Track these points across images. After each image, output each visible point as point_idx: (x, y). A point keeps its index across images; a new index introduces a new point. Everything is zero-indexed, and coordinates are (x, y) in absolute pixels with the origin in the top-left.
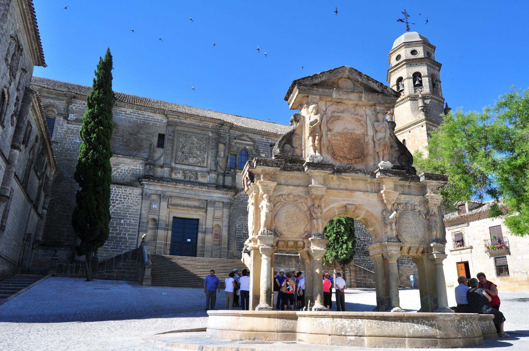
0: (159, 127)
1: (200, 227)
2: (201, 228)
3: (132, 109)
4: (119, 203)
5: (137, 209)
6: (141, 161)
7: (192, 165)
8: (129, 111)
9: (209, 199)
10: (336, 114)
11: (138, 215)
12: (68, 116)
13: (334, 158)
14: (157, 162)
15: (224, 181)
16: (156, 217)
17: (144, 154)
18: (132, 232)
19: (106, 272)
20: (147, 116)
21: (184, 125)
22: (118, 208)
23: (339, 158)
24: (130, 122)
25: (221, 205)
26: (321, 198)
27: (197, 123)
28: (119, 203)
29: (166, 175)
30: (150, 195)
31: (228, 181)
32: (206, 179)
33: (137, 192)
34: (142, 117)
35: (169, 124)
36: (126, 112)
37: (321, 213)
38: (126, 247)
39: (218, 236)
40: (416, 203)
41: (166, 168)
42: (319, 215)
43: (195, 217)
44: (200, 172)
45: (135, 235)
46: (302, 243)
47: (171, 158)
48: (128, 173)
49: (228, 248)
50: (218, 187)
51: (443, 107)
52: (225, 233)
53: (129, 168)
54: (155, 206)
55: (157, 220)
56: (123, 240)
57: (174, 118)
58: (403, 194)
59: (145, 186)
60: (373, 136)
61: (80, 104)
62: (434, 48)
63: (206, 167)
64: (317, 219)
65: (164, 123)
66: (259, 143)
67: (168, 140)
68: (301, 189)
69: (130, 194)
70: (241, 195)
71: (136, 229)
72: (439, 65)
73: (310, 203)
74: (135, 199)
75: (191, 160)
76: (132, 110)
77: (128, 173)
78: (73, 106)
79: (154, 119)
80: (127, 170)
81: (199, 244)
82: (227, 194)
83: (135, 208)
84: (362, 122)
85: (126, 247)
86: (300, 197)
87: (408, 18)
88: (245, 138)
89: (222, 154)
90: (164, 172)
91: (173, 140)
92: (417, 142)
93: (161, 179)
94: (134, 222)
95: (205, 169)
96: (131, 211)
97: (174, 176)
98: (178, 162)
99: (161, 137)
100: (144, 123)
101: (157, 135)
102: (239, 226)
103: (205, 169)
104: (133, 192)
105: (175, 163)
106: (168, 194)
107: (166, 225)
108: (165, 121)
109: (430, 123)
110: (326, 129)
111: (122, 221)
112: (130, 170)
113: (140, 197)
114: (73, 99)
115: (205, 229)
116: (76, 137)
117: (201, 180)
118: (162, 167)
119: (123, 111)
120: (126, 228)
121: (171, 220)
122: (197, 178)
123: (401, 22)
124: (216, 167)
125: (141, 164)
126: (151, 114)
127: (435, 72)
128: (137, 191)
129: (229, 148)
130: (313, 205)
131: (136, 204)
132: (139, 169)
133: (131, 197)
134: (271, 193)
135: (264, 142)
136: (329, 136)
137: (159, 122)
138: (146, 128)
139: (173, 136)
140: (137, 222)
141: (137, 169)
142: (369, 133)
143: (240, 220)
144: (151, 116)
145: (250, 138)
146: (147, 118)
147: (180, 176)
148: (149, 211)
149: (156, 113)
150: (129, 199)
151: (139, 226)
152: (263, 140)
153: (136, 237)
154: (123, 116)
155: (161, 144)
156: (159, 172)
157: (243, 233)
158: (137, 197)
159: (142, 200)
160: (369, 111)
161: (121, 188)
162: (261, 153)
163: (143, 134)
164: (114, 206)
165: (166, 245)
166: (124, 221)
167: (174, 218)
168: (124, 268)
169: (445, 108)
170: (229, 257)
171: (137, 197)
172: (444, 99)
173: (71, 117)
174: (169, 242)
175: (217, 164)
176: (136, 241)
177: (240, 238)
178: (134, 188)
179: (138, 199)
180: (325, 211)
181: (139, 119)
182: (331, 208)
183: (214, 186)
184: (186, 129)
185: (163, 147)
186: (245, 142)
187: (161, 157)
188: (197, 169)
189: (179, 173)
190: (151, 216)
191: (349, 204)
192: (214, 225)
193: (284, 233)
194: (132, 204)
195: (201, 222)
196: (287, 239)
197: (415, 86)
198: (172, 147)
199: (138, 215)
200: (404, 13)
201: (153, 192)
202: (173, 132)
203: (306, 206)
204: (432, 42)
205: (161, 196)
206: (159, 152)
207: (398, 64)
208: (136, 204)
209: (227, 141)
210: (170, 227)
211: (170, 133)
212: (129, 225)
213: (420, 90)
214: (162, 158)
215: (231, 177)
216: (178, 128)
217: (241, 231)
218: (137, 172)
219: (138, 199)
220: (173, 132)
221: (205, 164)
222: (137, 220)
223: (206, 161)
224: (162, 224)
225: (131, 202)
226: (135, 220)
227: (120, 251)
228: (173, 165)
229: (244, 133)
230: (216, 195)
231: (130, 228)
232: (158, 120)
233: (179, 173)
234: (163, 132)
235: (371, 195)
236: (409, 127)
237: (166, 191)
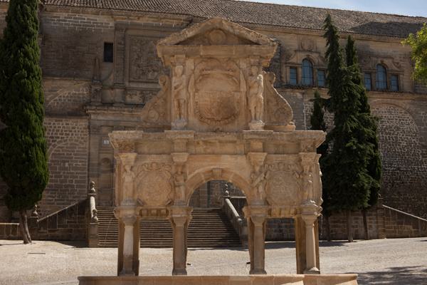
3: (67, 12)
4: (61, 142)
6: (84, 83)
7: (153, 82)
8: (63, 15)
10: (205, 72)
13: (201, 121)
19: (50, 231)
20: (88, 19)
22: (59, 147)
23: (206, 120)
24: (65, 31)
26: (184, 166)
27: (154, 23)
28: (61, 142)
29: (118, 99)
33: (82, 125)
34: (81, 22)
35: (117, 28)
36: (59, 17)
37: (185, 180)
38: (74, 197)
40: (291, 163)
41: (117, 90)
42: (182, 182)
45: (84, 182)
46: (165, 211)
47: (124, 75)
49: (209, 193)
53: (69, 93)
56: (70, 189)
57: (123, 19)
58: (275, 154)
59: (92, 117)
60: (246, 92)
64: (179, 186)
65: (111, 27)
67: (118, 50)
68: (164, 156)
69: (73, 128)
71: (85, 173)
73: (173, 171)
75: (150, 75)
76: (66, 15)
80: (67, 96)
84: (234, 78)
85: (74, 197)
86: (164, 164)
96: (77, 151)
97: (128, 100)
98: (132, 79)
99: (108, 46)
101: (103, 45)
104: (76, 125)
105: (130, 82)
108: (112, 24)
110: (194, 90)
111: (67, 165)
112: (71, 97)
118: (112, 88)
119: (55, 17)
120: (72, 173)
125: (85, 86)
126: (92, 17)
128: (82, 123)
130: (177, 173)
132: (83, 94)
133: (75, 131)
134: (132, 163)
136: (196, 97)
139: (124, 44)
141: (79, 94)
142: (242, 90)
146: (87, 22)
148: (100, 150)
149: (98, 14)
150: (72, 134)
151: (88, 170)
154: (55, 24)
155: (108, 58)
156: (110, 95)
158: (82, 132)
159: (90, 134)
160: (244, 64)
161: (62, 121)
164: (54, 146)
166: (69, 165)
168: (71, 226)
170: (211, 203)
171: (82, 132)
180: (189, 177)
181: (77, 25)
182: (196, 175)
184: (141, 33)
185: (112, 62)
187: (110, 75)
190: (103, 156)
191: (214, 169)
193: (147, 202)
194: (77, 141)
196: (149, 208)
198: (124, 59)
201: (103, 123)
202: (124, 38)
203: (169, 174)
206: (107, 69)
208: (82, 140)
212: (76, 168)
214: (112, 76)
216: (129, 32)
220: (124, 38)
226: (83, 162)
228: (127, 84)
233: (136, 95)
234: (110, 40)
235: (239, 157)
237: (120, 121)
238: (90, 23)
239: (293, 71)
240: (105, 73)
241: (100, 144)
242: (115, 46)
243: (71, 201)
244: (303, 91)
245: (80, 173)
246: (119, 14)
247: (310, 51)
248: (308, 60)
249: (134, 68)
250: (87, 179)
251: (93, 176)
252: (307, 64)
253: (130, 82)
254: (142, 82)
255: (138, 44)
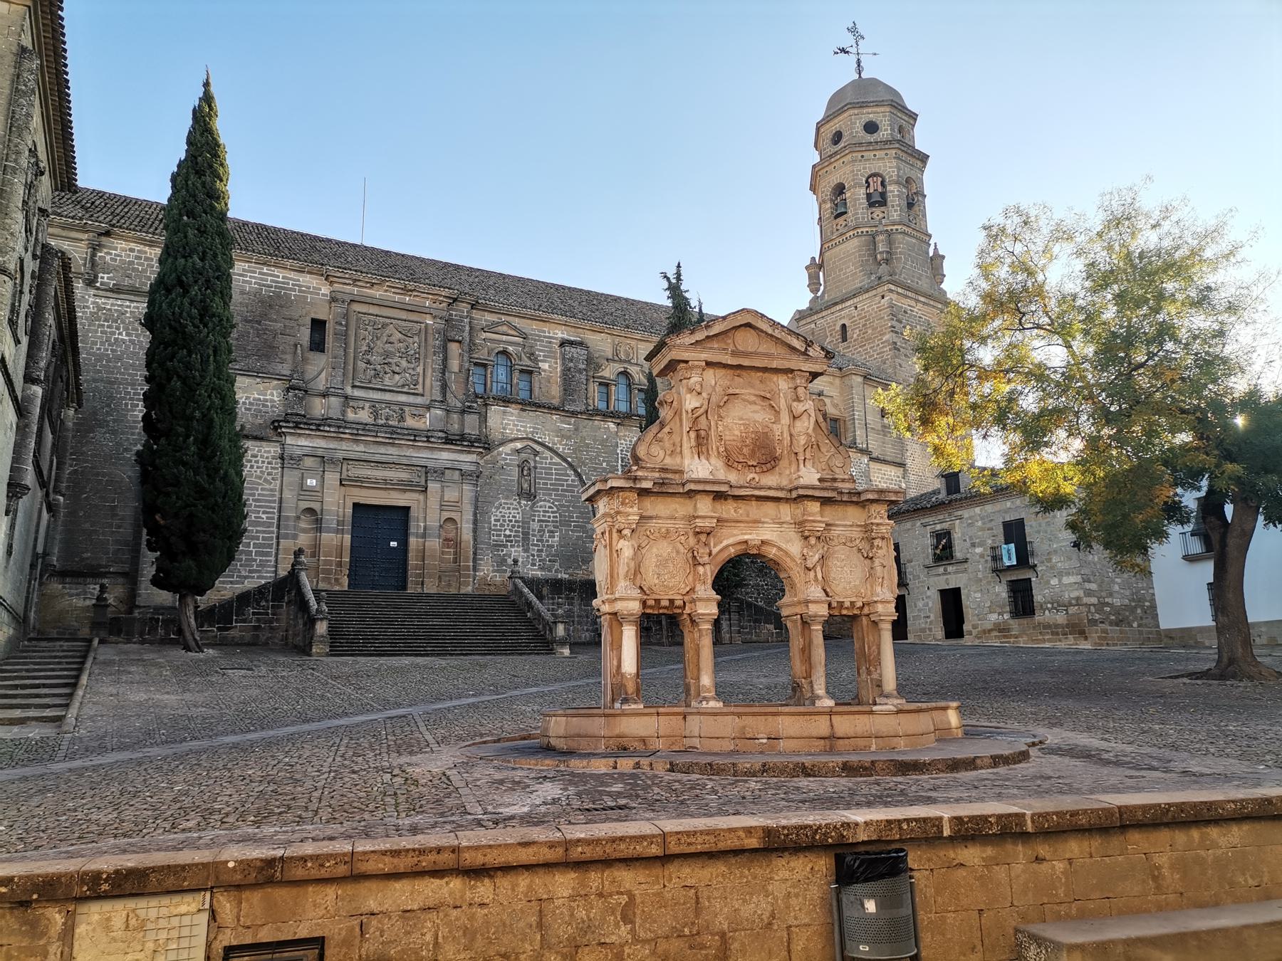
0: (311, 304)
1: (412, 524)
2: (416, 526)
5: (271, 490)
7: (390, 391)
9: (430, 464)
11: (274, 502)
12: (96, 277)
14: (311, 385)
15: (462, 423)
16: (316, 506)
17: (280, 366)
18: (264, 539)
20: (283, 278)
21: (369, 300)
25: (456, 475)
30: (300, 459)
31: (471, 425)
32: (423, 420)
33: (269, 452)
34: (272, 281)
38: (250, 572)
39: (453, 543)
41: (332, 399)
43: (402, 503)
44: (410, 405)
45: (270, 546)
48: (246, 409)
50: (449, 441)
51: (928, 253)
52: (467, 535)
54: (311, 482)
55: (319, 513)
61: (123, 250)
62: (913, 117)
63: (423, 395)
65: (323, 295)
66: (535, 340)
70: (500, 454)
71: (272, 532)
72: (924, 158)
74: (267, 468)
77: (246, 409)
78: (106, 253)
79: (299, 286)
81: (412, 561)
82: (469, 452)
83: (267, 487)
85: (250, 572)
87: (861, 42)
88: (505, 328)
89: (454, 364)
90: (329, 408)
91: (346, 334)
92: (870, 331)
93: (319, 425)
94: (267, 518)
95: (419, 400)
97: (351, 416)
100: (278, 296)
102: (495, 520)
103: (419, 400)
106: (340, 455)
107: (338, 521)
109: (900, 290)
112: (250, 404)
113: (276, 463)
114: (104, 239)
115: (425, 528)
116: (118, 328)
117: (410, 422)
121: (349, 511)
122: (402, 419)
123: (843, 54)
124: (444, 395)
126: (292, 275)
127: (913, 174)
128: (271, 450)
129: (471, 350)
131: (269, 478)
133: (257, 462)
135: (545, 337)
137: (311, 293)
138: (281, 306)
139: (346, 326)
140: (273, 518)
141: (266, 400)
143: (498, 508)
144: (291, 279)
145: (515, 328)
146: (283, 283)
147: (364, 416)
150: (252, 467)
151: (278, 527)
152: (544, 332)
153: (274, 551)
155: (318, 345)
156: (318, 408)
157: (505, 535)
158: (269, 463)
159: (283, 468)
162: (542, 361)
163: (275, 321)
165: (340, 564)
167: (356, 505)
169: (931, 254)
171: (269, 463)
172: (930, 236)
173: (104, 278)
174: (346, 559)
175: (444, 387)
176: (273, 559)
177: (500, 546)
178: (264, 444)
179: (272, 468)
181: (264, 285)
183: (441, 434)
185: (323, 351)
186: (504, 338)
188: (403, 398)
189: (363, 408)
192: (443, 520)
194: (260, 478)
195: (413, 513)
197: (871, 205)
199: (274, 502)
200: (853, 30)
201: (306, 451)
202: (346, 316)
204: (911, 105)
205: (325, 461)
207: (836, 153)
208: (269, 478)
209: (466, 334)
210: (348, 527)
211: (339, 319)
213: (881, 215)
214: (323, 374)
215: (476, 417)
217: (501, 530)
218: (267, 406)
219: (272, 468)
220: (346, 316)
221: (420, 387)
222: (274, 513)
223: (421, 380)
224: (330, 520)
225: (258, 473)
227: (237, 583)
228: (349, 390)
229: (504, 318)
230: (445, 455)
231: (257, 531)
232: (309, 288)
234: (321, 317)
236: (854, 296)
238: (288, 284)
239: (603, 389)
240: (311, 370)
241: (302, 486)
242: (330, 328)
243: (246, 577)
244: (618, 421)
245: (264, 532)
246: (339, 275)
247: (629, 362)
248: (625, 374)
249: (361, 365)
250: (275, 540)
251: (286, 537)
252: (622, 380)
253: (354, 387)
254: (373, 389)
255: (370, 328)
